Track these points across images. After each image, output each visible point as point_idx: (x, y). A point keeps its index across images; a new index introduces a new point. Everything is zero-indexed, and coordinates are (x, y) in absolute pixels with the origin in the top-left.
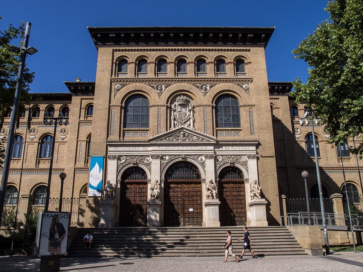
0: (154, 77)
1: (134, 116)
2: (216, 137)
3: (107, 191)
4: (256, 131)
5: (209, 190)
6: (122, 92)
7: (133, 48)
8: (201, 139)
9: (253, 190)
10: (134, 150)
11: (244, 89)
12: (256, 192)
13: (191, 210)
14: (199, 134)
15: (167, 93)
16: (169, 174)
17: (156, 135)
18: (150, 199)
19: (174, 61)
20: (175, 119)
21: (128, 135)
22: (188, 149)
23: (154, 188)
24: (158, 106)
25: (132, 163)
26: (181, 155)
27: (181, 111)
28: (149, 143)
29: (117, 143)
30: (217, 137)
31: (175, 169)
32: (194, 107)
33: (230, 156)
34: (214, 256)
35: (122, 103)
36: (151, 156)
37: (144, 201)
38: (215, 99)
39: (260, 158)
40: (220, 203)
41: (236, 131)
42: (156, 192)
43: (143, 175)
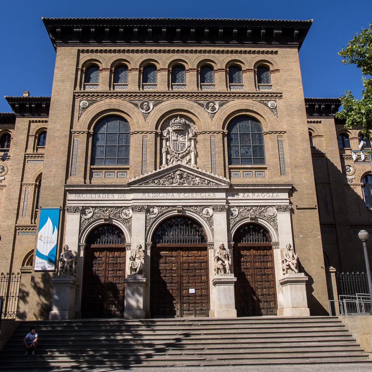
0: (137, 90)
1: (107, 148)
2: (229, 180)
3: (64, 262)
4: (288, 170)
5: (219, 259)
6: (90, 113)
7: (108, 48)
8: (206, 182)
9: (285, 259)
10: (106, 199)
11: (269, 108)
12: (290, 263)
13: (192, 291)
14: (204, 175)
16: (159, 236)
17: (139, 176)
18: (130, 274)
19: (167, 67)
20: (167, 153)
21: (97, 177)
22: (188, 198)
23: (135, 258)
24: (143, 132)
25: (102, 219)
26: (176, 206)
27: (177, 140)
28: (129, 188)
29: (80, 188)
30: (230, 180)
31: (167, 228)
32: (196, 135)
33: (250, 208)
34: (228, 365)
35: (89, 128)
36: (132, 208)
37: (120, 277)
38: (228, 123)
39: (295, 210)
40: (236, 280)
41: (258, 170)
42: (139, 263)
43: (120, 237)
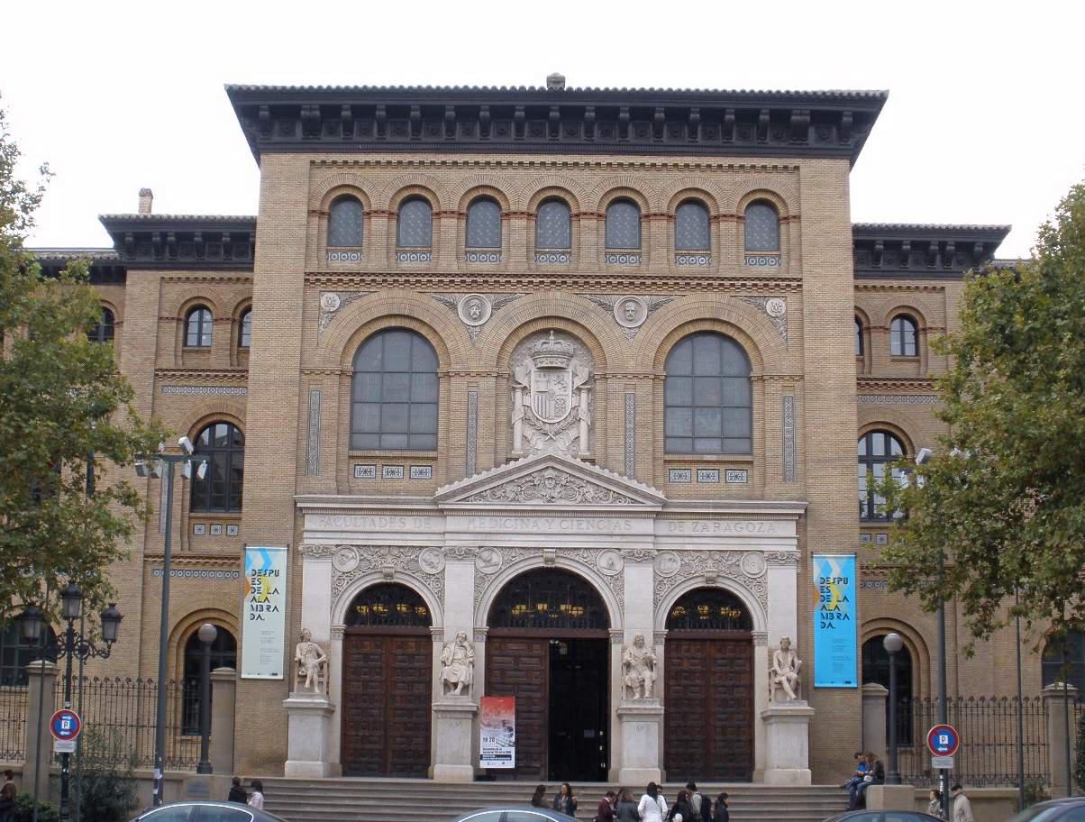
12: (784, 679)
15: (495, 331)
24: (468, 374)
